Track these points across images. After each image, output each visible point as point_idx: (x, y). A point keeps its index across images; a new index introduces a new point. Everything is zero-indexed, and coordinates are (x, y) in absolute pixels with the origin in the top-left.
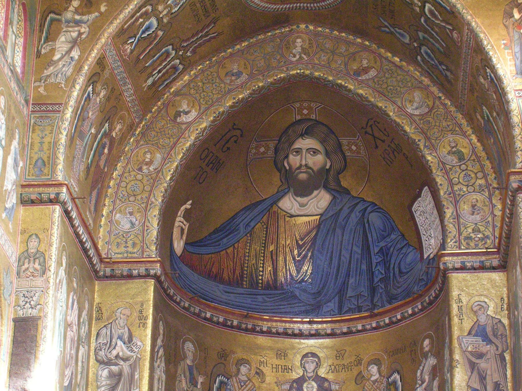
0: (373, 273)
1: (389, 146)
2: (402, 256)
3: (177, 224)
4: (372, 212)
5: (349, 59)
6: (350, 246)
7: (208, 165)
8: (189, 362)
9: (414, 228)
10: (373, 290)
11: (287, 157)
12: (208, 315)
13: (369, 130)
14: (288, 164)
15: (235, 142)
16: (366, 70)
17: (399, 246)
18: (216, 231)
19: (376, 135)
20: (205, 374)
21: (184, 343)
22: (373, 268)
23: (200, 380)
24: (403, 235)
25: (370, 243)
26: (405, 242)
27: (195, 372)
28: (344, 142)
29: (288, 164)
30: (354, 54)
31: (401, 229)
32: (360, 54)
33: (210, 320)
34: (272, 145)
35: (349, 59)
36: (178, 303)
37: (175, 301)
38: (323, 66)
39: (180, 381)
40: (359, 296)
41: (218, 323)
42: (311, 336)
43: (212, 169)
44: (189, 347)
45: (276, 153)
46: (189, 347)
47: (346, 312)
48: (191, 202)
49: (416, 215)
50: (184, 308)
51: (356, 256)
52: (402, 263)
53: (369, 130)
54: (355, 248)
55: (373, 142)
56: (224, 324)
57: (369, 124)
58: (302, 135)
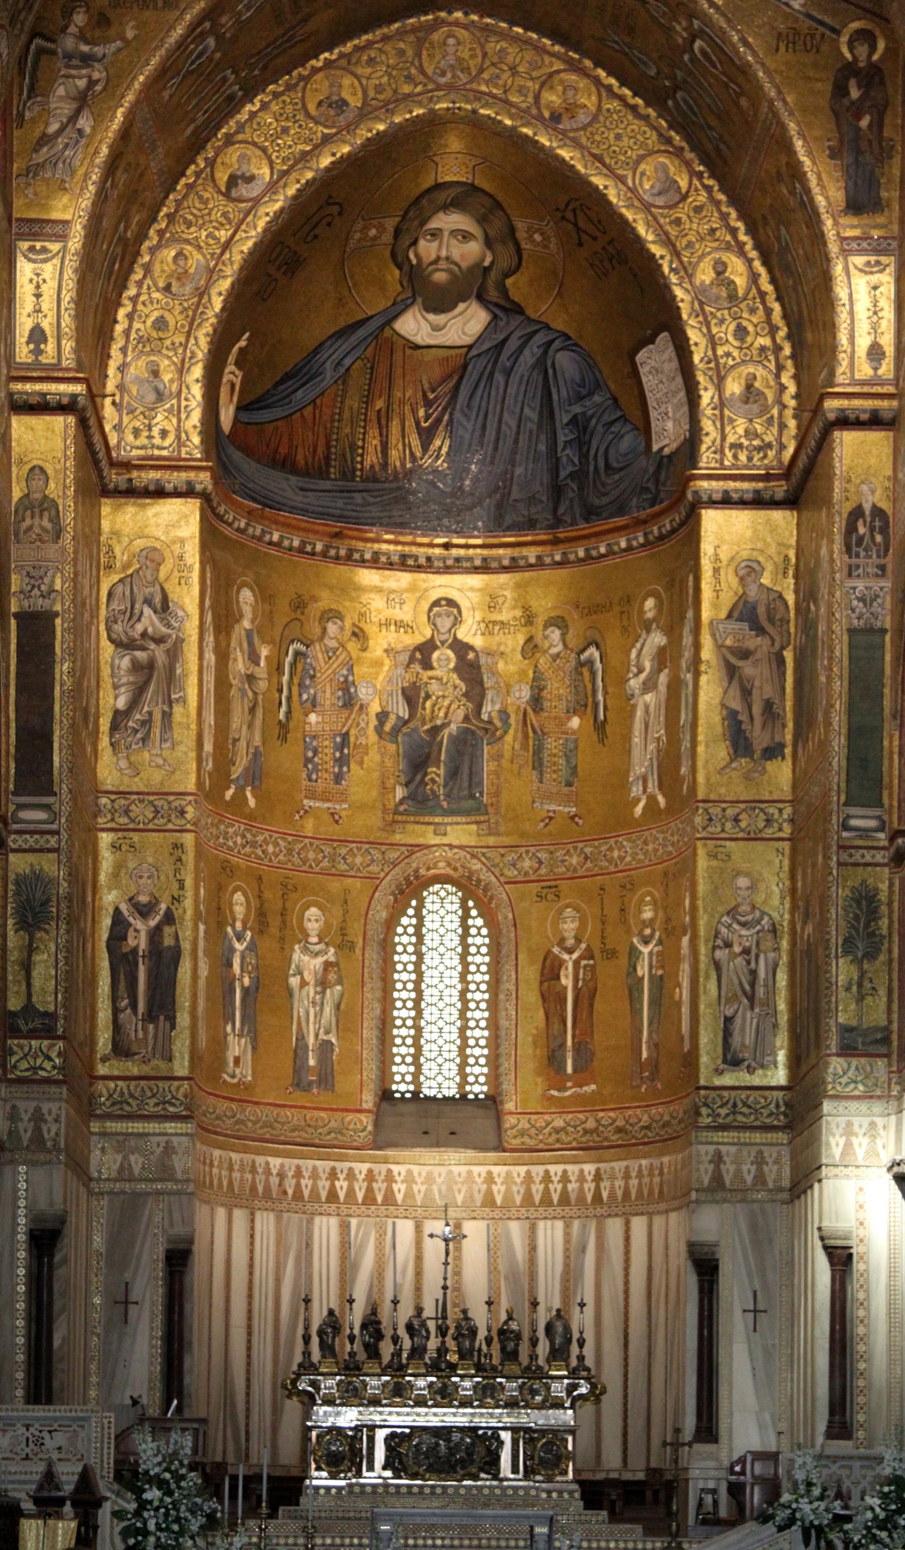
0: (558, 459)
1: (603, 248)
2: (611, 437)
3: (225, 380)
4: (562, 349)
5: (543, 85)
6: (519, 405)
7: (279, 268)
8: (246, 624)
9: (636, 392)
10: (557, 491)
11: (415, 243)
12: (276, 537)
13: (569, 215)
14: (417, 255)
15: (329, 224)
16: (571, 109)
17: (607, 418)
18: (287, 377)
19: (581, 223)
20: (271, 642)
21: (238, 592)
22: (559, 449)
23: (264, 652)
24: (615, 400)
25: (555, 404)
26: (619, 414)
27: (256, 640)
28: (521, 226)
29: (417, 255)
30: (551, 75)
31: (613, 387)
32: (562, 75)
33: (278, 545)
34: (390, 224)
35: (543, 85)
36: (230, 525)
37: (226, 522)
38: (494, 96)
39: (235, 660)
40: (532, 500)
41: (290, 549)
42: (447, 570)
43: (285, 274)
44: (246, 596)
45: (396, 237)
46: (246, 596)
47: (508, 529)
48: (247, 335)
49: (643, 370)
50: (238, 530)
51: (529, 425)
52: (612, 452)
53: (569, 215)
54: (527, 410)
55: (575, 236)
56: (301, 550)
57: (571, 207)
58: (445, 208)
